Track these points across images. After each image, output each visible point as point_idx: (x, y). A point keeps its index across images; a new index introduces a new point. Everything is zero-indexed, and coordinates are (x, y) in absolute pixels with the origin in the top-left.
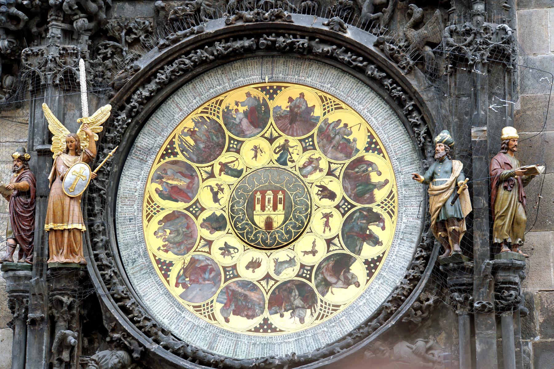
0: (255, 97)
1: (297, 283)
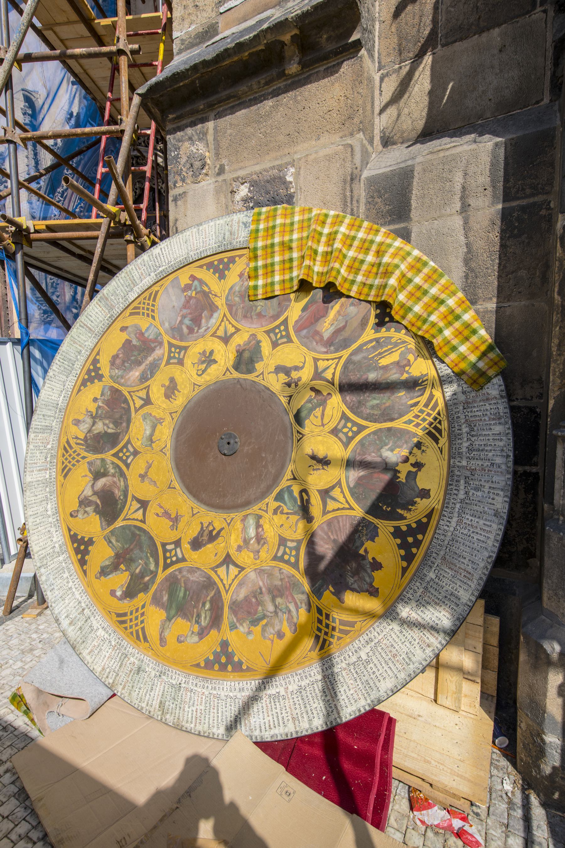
0: (414, 503)
1: (121, 437)
